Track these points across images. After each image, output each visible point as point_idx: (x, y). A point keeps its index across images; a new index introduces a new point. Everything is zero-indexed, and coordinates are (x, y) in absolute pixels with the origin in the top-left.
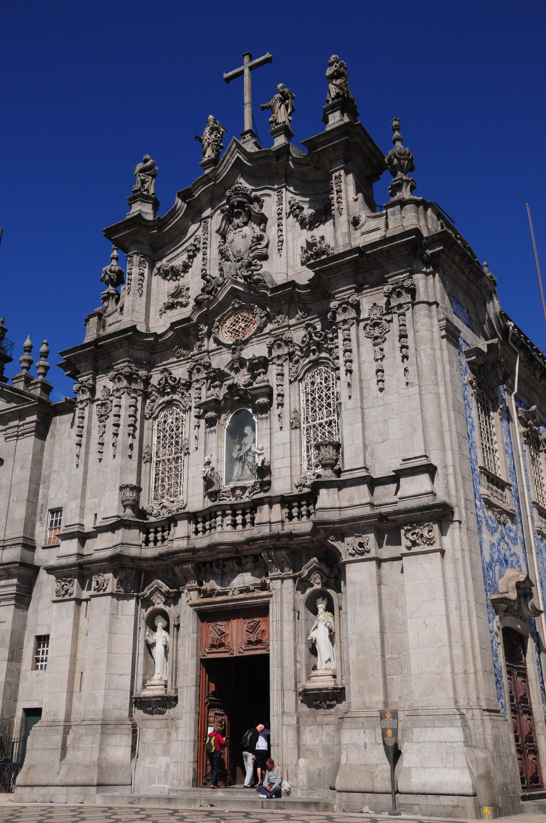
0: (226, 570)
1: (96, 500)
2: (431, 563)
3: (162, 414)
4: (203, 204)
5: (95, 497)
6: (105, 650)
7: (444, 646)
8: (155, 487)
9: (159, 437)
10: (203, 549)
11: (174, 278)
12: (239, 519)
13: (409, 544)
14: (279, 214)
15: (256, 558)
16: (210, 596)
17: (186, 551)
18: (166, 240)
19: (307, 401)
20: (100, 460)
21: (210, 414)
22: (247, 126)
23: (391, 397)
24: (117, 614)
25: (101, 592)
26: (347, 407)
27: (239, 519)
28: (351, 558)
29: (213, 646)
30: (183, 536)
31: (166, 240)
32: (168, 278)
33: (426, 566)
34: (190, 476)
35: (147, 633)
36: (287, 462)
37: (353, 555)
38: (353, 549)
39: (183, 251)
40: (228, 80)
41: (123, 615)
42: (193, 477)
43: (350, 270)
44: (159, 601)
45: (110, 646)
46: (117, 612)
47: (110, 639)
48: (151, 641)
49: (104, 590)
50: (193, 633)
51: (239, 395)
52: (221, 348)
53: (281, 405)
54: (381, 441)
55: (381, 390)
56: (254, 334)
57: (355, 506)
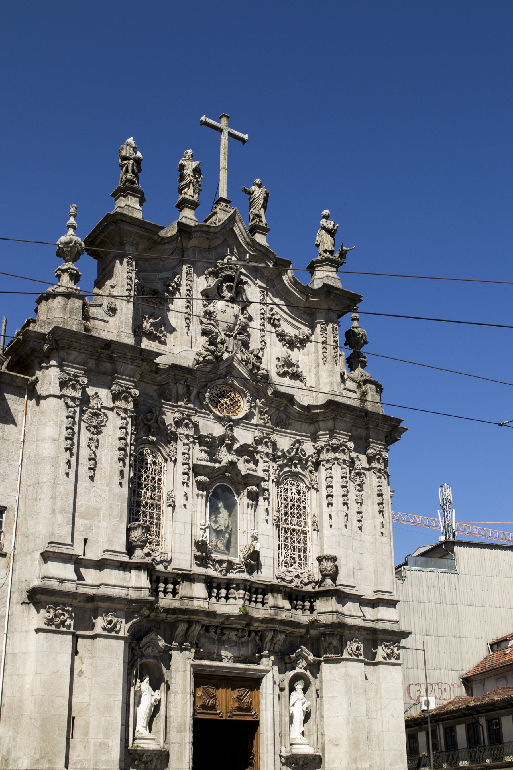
0: (225, 638)
1: (87, 522)
2: (396, 673)
7: (403, 732)
13: (385, 655)
14: (263, 314)
19: (282, 503)
20: (92, 478)
21: (202, 478)
22: (223, 193)
23: (366, 536)
25: (113, 634)
28: (349, 657)
30: (204, 597)
33: (394, 674)
37: (351, 655)
38: (351, 650)
39: (159, 279)
42: (180, 534)
43: (350, 420)
49: (117, 632)
52: (209, 415)
54: (358, 568)
55: (360, 528)
56: (241, 419)
57: (353, 616)
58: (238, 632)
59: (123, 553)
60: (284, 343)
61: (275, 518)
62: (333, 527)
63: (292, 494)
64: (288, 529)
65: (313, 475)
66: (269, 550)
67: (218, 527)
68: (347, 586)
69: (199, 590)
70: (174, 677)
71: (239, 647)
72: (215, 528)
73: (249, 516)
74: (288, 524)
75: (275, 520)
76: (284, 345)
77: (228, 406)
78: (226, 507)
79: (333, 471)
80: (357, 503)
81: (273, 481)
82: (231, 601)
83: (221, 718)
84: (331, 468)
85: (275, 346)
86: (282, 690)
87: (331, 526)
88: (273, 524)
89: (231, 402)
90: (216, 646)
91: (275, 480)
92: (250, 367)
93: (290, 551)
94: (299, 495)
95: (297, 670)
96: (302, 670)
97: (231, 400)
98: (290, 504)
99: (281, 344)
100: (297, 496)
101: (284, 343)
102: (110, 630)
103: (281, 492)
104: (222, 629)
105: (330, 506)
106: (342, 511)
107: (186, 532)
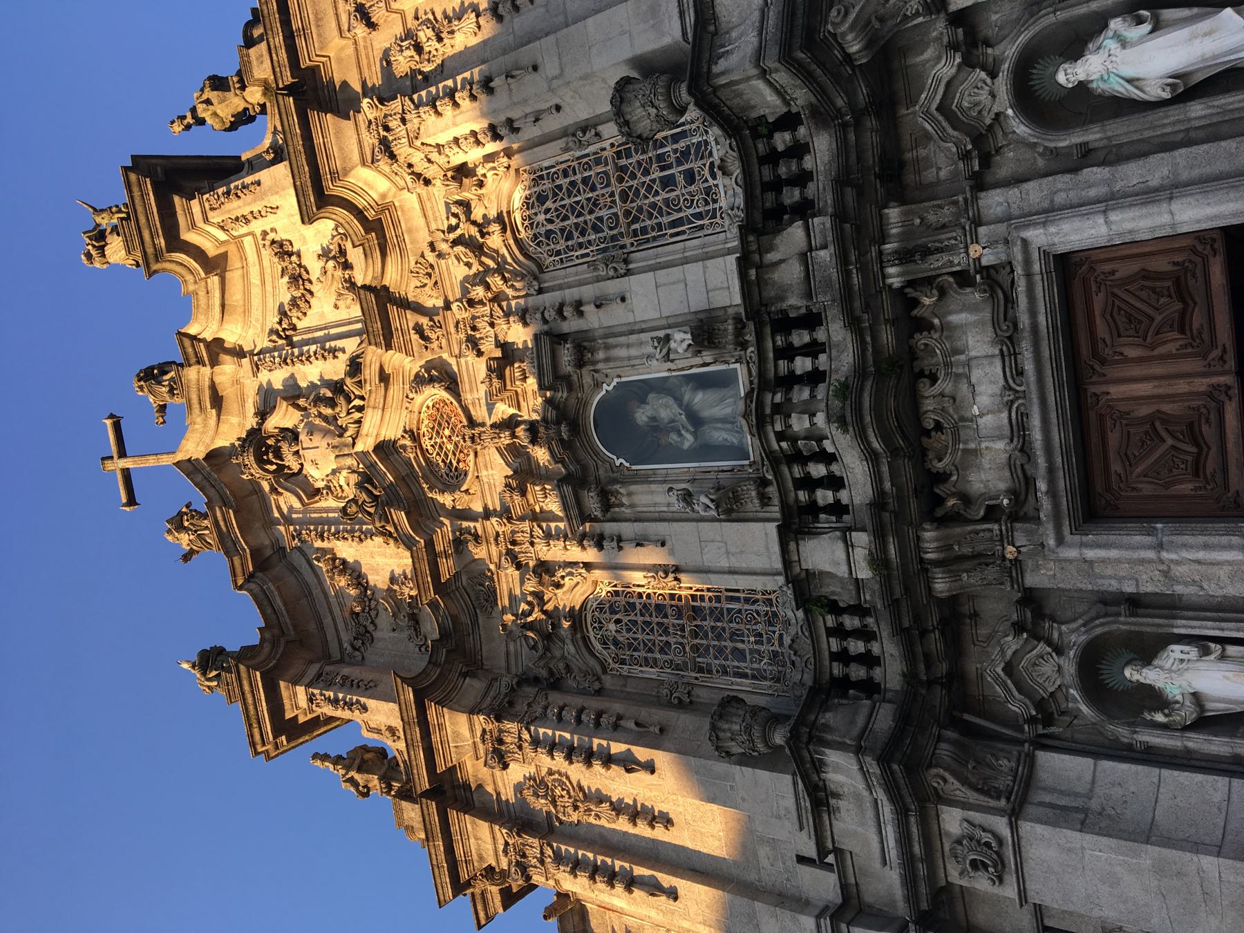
3: (598, 646)
4: (267, 542)
5: (756, 855)
6: (1209, 863)
8: (754, 677)
9: (646, 662)
10: (877, 478)
11: (373, 613)
12: (802, 365)
15: (906, 300)
16: (1029, 482)
17: (879, 535)
18: (312, 627)
19: (581, 246)
21: (592, 502)
24: (1085, 811)
26: (557, 72)
27: (802, 365)
29: (1197, 469)
31: (312, 627)
32: (371, 628)
34: (724, 563)
35: (1160, 718)
36: (693, 271)
40: (132, 501)
41: (1089, 795)
42: (728, 553)
44: (1048, 668)
45: (1197, 847)
46: (1077, 810)
47: (1168, 842)
48: (1188, 713)
50: (1151, 532)
51: (558, 423)
53: (578, 306)
58: (921, 374)
59: (795, 784)
60: (308, 296)
61: (611, 273)
62: (557, 101)
63: (550, 221)
64: (627, 213)
65: (484, 175)
66: (689, 277)
67: (687, 430)
68: (682, 14)
69: (823, 554)
70: (1113, 582)
71: (968, 364)
72: (690, 437)
73: (633, 352)
74: (616, 214)
75: (615, 269)
76: (311, 293)
77: (453, 431)
78: (643, 401)
79: (443, 138)
80: (479, 27)
81: (540, 291)
82: (830, 449)
83: (1235, 392)
84: (439, 147)
85: (322, 315)
86: (1086, 156)
87: (558, 108)
88: (628, 273)
89: (444, 424)
90: (983, 445)
91: (536, 285)
92: (357, 415)
93: (672, 195)
94: (547, 198)
95: (1004, 102)
96: (1002, 85)
97: (440, 424)
98: (573, 220)
99: (313, 301)
100: (549, 204)
101: (308, 296)
102: (1000, 863)
103: (558, 253)
104: (927, 433)
105: (516, 125)
106: (510, 90)
107: (719, 539)
